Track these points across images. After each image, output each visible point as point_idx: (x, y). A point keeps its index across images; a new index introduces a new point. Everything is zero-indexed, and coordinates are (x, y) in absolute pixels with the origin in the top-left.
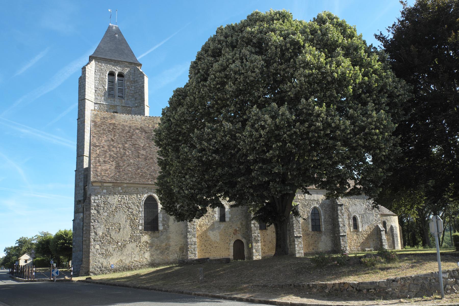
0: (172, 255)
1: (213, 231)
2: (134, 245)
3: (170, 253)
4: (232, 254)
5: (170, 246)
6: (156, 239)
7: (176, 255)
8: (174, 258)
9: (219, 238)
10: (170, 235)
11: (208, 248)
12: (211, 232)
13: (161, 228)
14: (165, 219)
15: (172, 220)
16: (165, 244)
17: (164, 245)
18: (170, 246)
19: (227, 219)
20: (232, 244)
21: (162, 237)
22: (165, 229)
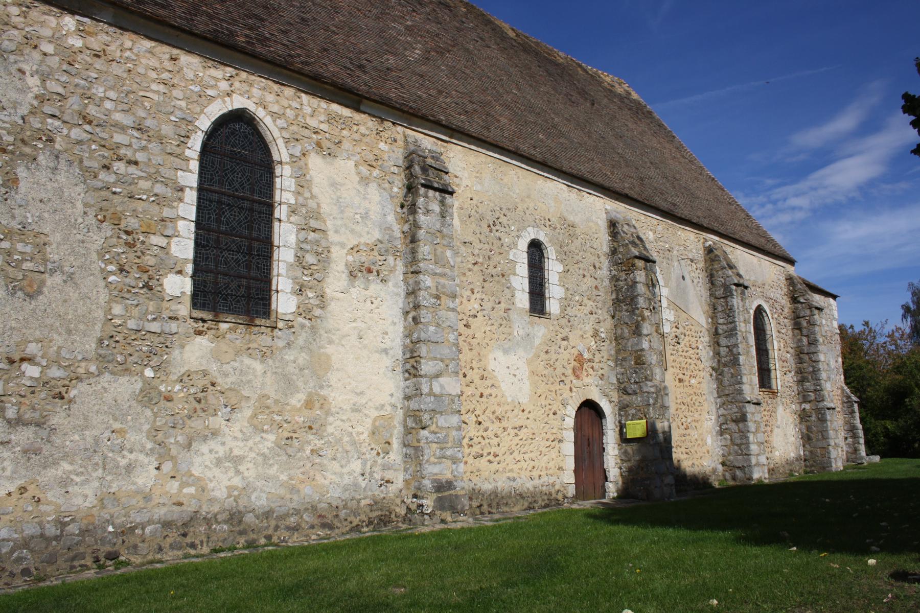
0: (335, 466)
1: (506, 352)
2: (124, 388)
3: (329, 453)
4: (570, 464)
5: (328, 413)
6: (258, 367)
7: (356, 466)
8: (347, 480)
9: (527, 387)
10: (330, 350)
11: (490, 433)
12: (499, 354)
13: (284, 302)
14: (310, 259)
15: (341, 267)
16: (301, 397)
17: (298, 399)
18: (328, 413)
19: (553, 306)
20: (570, 422)
21: (290, 356)
22: (304, 311)
